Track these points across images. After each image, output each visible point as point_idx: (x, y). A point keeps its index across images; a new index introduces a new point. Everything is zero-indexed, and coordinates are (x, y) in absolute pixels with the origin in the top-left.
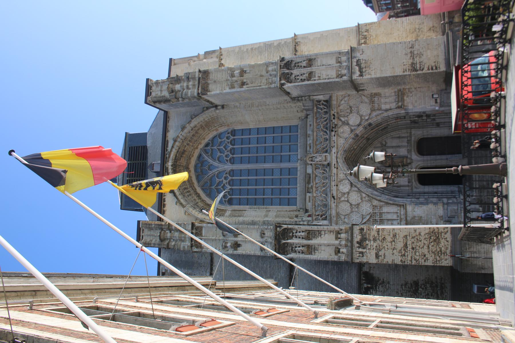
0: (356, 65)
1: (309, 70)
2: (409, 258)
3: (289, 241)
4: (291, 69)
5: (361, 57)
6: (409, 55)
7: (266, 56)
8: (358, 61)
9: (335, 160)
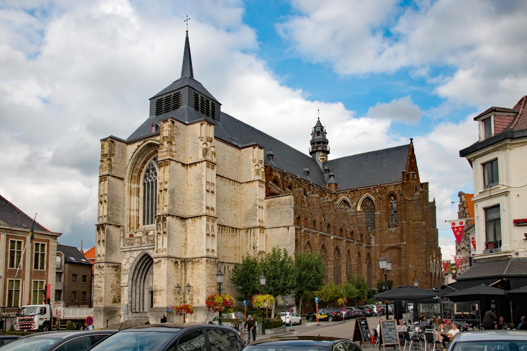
0: (159, 260)
1: (162, 233)
3: (101, 231)
4: (163, 222)
5: (162, 263)
6: (161, 289)
8: (161, 261)
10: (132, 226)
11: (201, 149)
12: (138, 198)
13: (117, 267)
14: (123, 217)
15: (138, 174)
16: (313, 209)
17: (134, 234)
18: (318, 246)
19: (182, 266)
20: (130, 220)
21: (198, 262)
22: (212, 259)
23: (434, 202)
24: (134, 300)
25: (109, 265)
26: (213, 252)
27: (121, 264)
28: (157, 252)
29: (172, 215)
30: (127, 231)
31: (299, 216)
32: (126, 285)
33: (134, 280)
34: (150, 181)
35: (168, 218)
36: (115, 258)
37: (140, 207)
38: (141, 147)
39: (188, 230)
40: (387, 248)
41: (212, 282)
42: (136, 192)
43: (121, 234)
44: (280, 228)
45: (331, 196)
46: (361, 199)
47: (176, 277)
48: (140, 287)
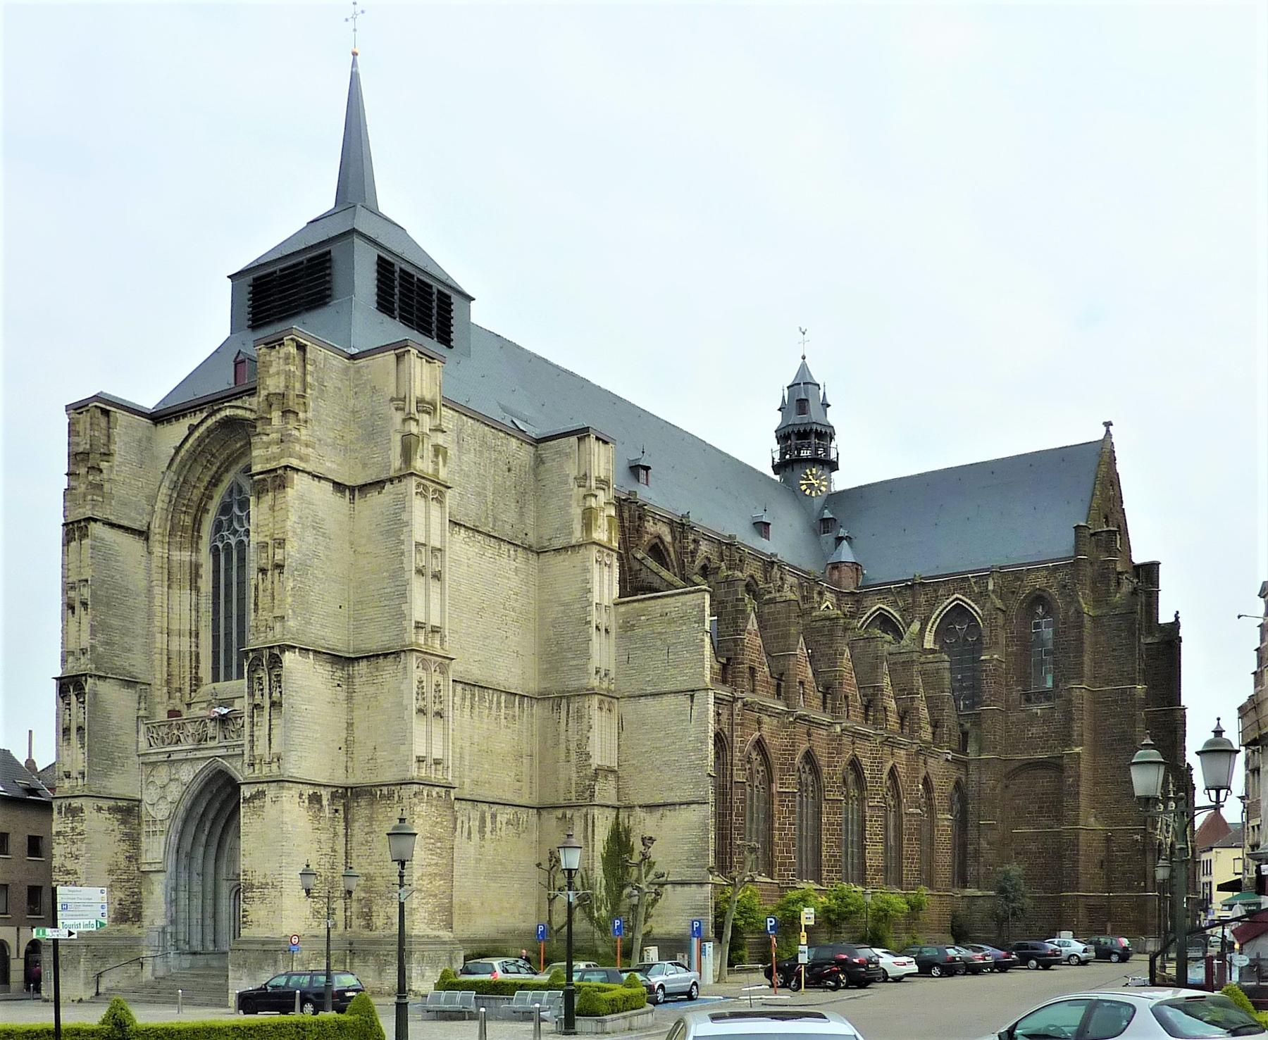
2: (58, 878)
6: (264, 881)
7: (386, 591)
9: (211, 755)
10: (175, 685)
11: (398, 437)
12: (194, 597)
13: (128, 811)
14: (149, 654)
15: (195, 517)
16: (776, 637)
17: (183, 708)
18: (789, 754)
19: (336, 811)
20: (168, 664)
21: (390, 796)
22: (437, 789)
23: (1175, 625)
24: (182, 915)
25: (101, 803)
26: (440, 767)
27: (140, 801)
28: (253, 765)
29: (301, 649)
30: (158, 700)
31: (728, 659)
32: (158, 867)
33: (182, 854)
34: (233, 541)
35: (288, 658)
36: (122, 784)
37: (202, 624)
38: (202, 429)
39: (358, 698)
40: (1017, 764)
41: (433, 862)
42: (188, 571)
43: (139, 709)
44: (665, 697)
45: (838, 600)
46: (937, 612)
47: (316, 846)
48: (203, 874)
